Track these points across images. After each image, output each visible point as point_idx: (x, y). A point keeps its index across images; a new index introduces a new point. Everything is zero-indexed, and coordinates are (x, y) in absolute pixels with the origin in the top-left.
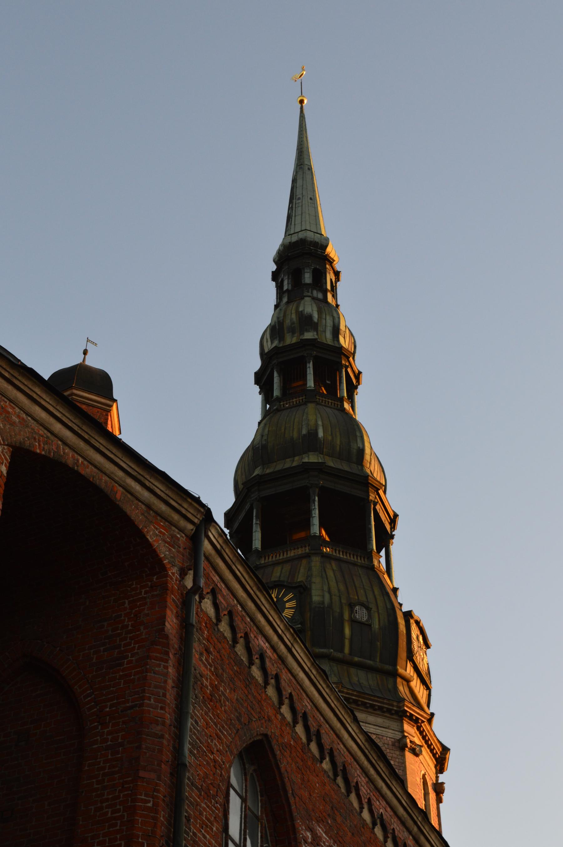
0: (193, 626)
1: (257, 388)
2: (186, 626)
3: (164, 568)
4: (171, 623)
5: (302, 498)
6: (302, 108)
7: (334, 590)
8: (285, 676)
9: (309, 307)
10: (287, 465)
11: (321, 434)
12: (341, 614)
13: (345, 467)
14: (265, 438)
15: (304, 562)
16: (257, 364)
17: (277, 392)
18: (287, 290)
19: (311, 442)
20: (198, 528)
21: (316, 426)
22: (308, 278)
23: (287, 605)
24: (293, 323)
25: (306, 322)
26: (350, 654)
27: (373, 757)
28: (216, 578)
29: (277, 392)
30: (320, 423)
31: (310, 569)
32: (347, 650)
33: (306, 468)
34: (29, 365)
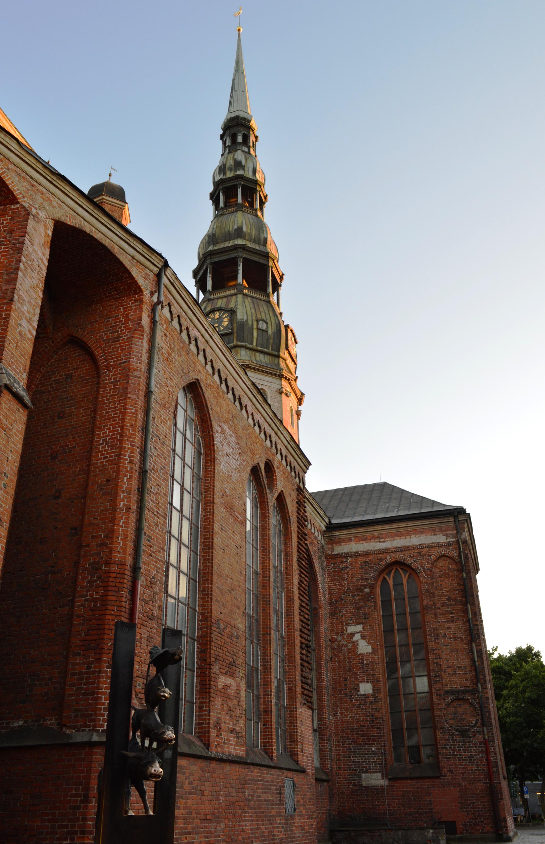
0: (157, 321)
1: (211, 202)
2: (153, 322)
3: (141, 291)
4: (145, 321)
5: (233, 262)
6: (239, 34)
7: (249, 313)
8: (208, 351)
9: (239, 156)
10: (226, 245)
11: (244, 229)
12: (252, 325)
13: (257, 247)
14: (214, 230)
15: (234, 297)
16: (211, 188)
17: (222, 204)
18: (228, 146)
19: (239, 233)
20: (160, 270)
21: (242, 223)
22: (240, 139)
23: (225, 320)
24: (231, 165)
25: (238, 165)
26: (256, 346)
27: (255, 392)
28: (171, 298)
29: (222, 204)
30: (244, 222)
31: (237, 301)
32: (255, 344)
33: (236, 247)
34: (62, 174)
